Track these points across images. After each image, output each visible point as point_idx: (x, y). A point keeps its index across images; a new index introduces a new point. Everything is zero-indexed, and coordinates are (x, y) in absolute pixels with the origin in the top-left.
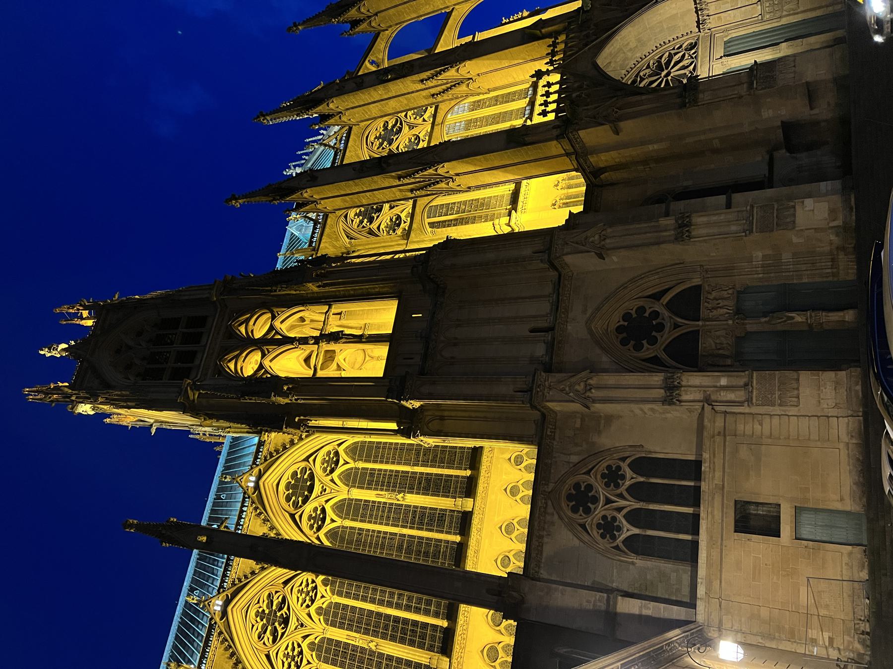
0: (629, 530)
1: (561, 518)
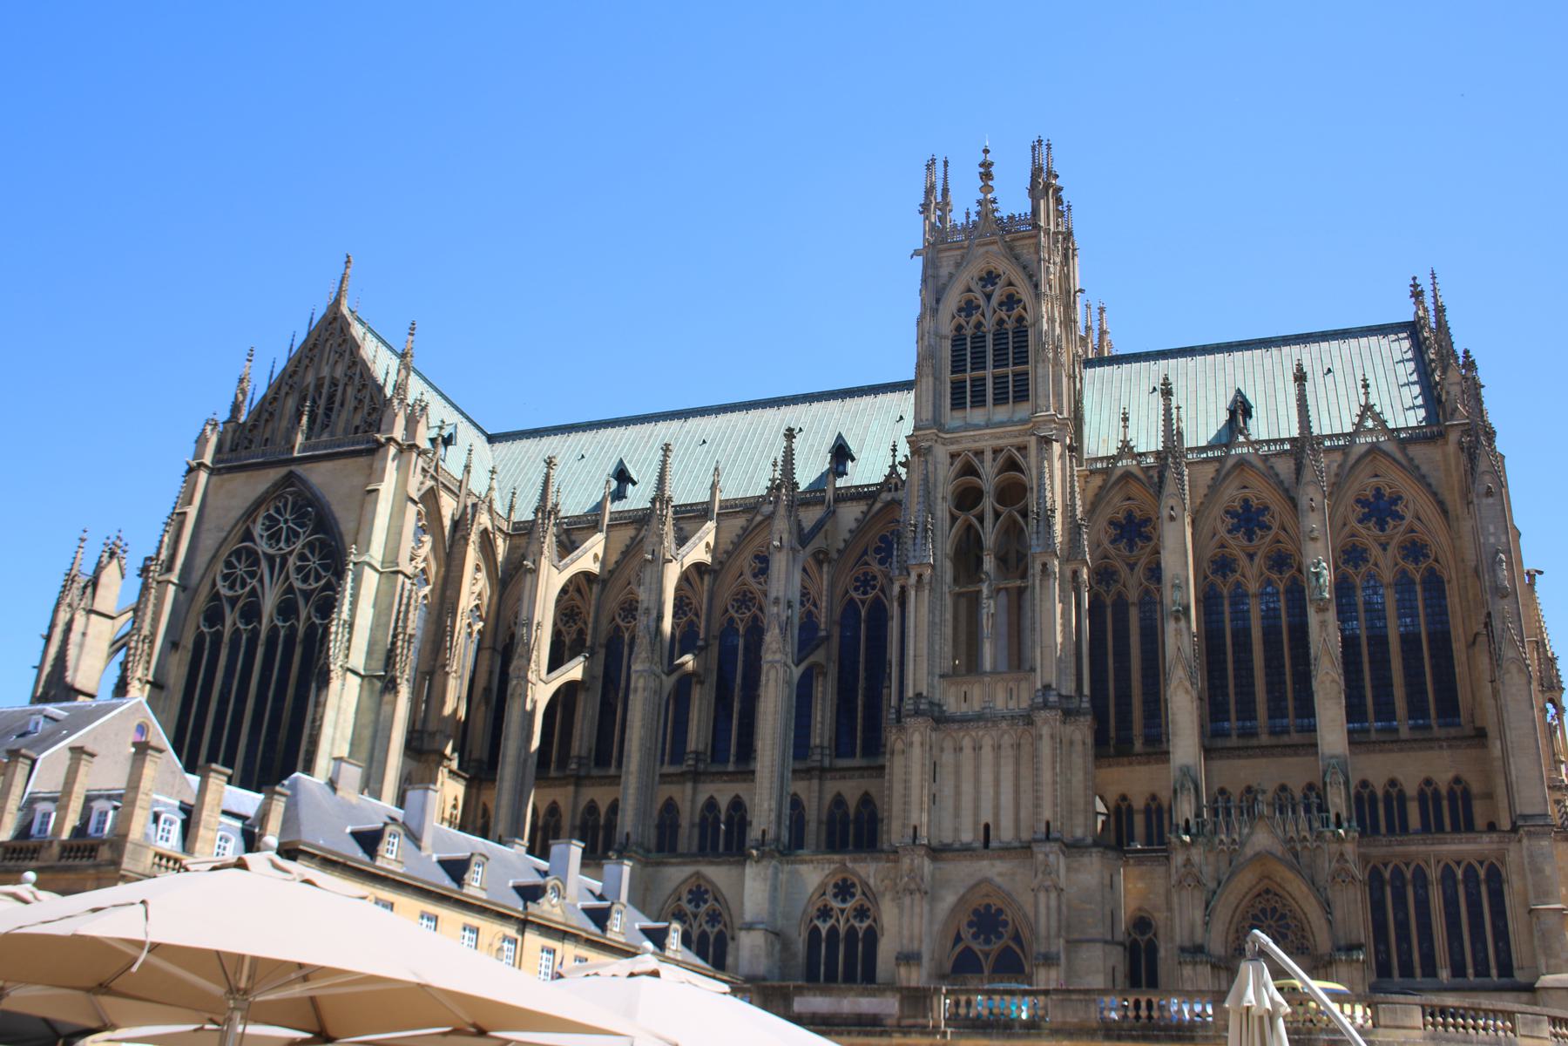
0: (824, 928)
1: (827, 876)
